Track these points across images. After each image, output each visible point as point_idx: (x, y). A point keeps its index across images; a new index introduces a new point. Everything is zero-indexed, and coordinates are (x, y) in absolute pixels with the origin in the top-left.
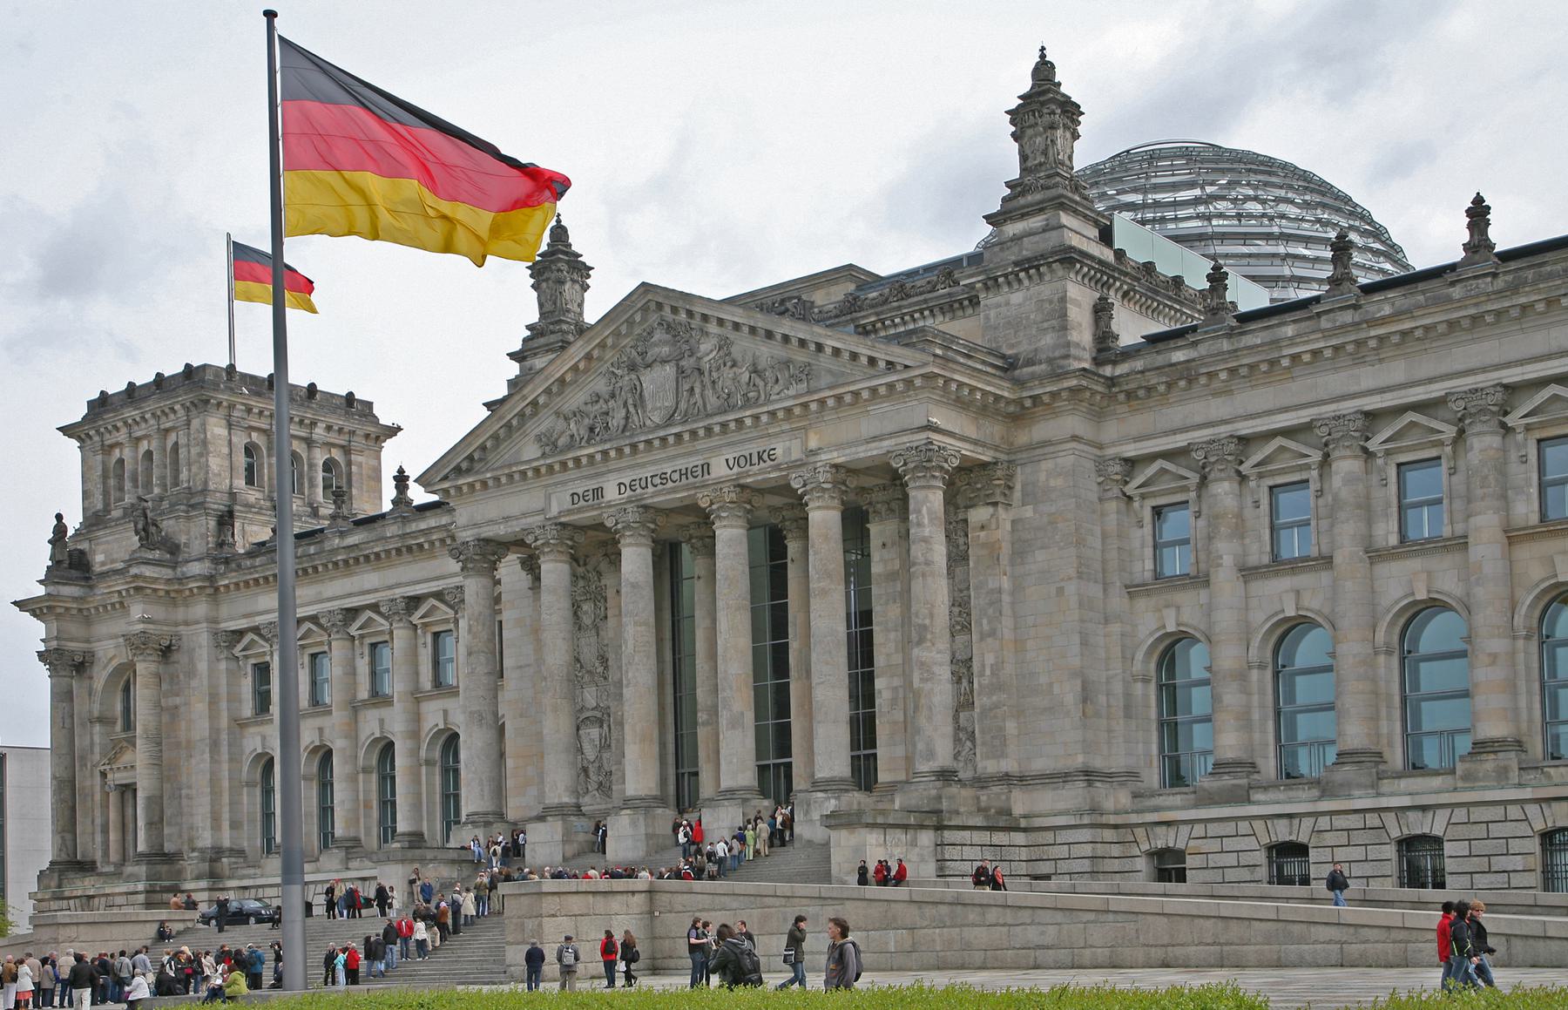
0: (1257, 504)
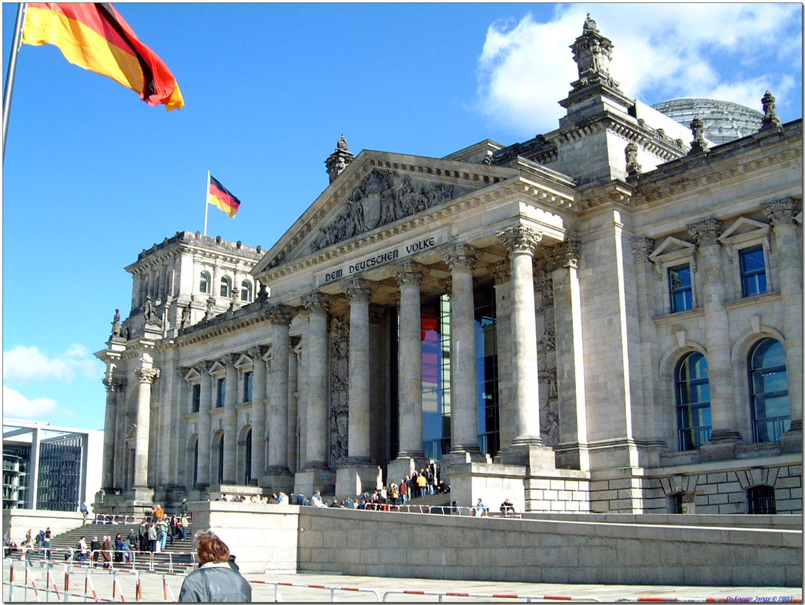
0: (731, 261)
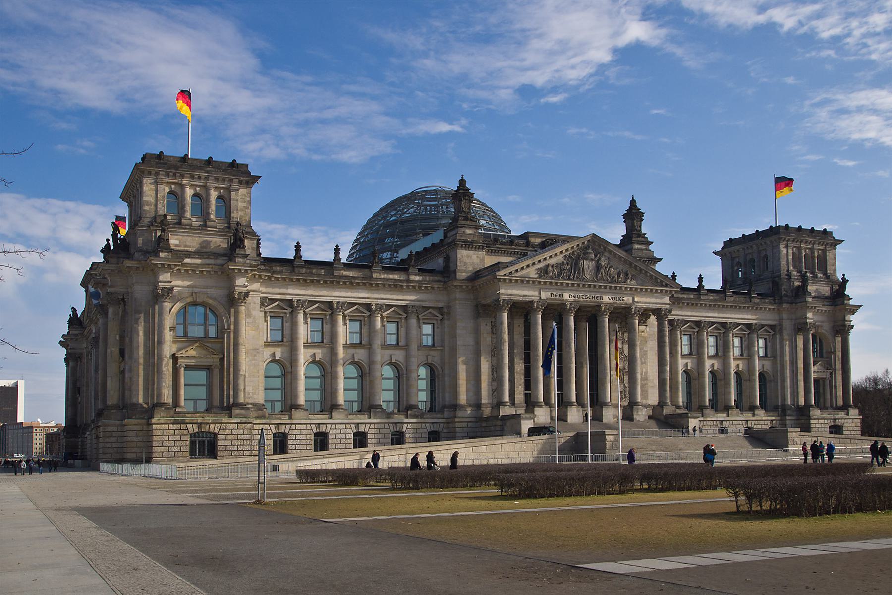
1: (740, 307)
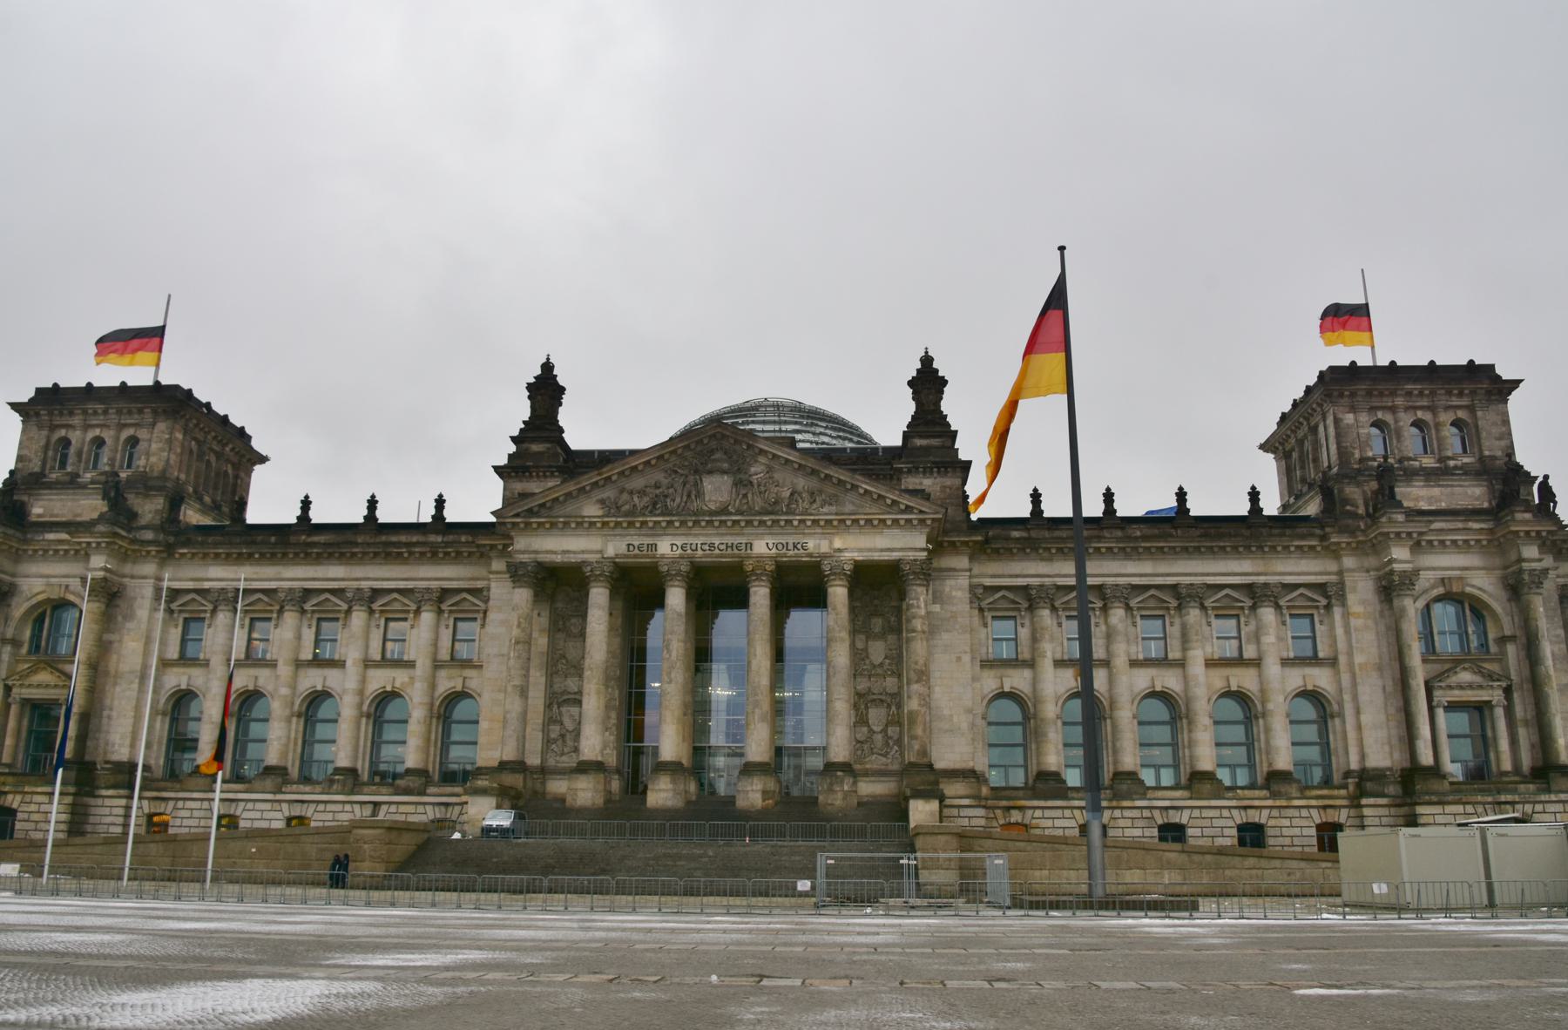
0: (1060, 625)
1: (1212, 547)
